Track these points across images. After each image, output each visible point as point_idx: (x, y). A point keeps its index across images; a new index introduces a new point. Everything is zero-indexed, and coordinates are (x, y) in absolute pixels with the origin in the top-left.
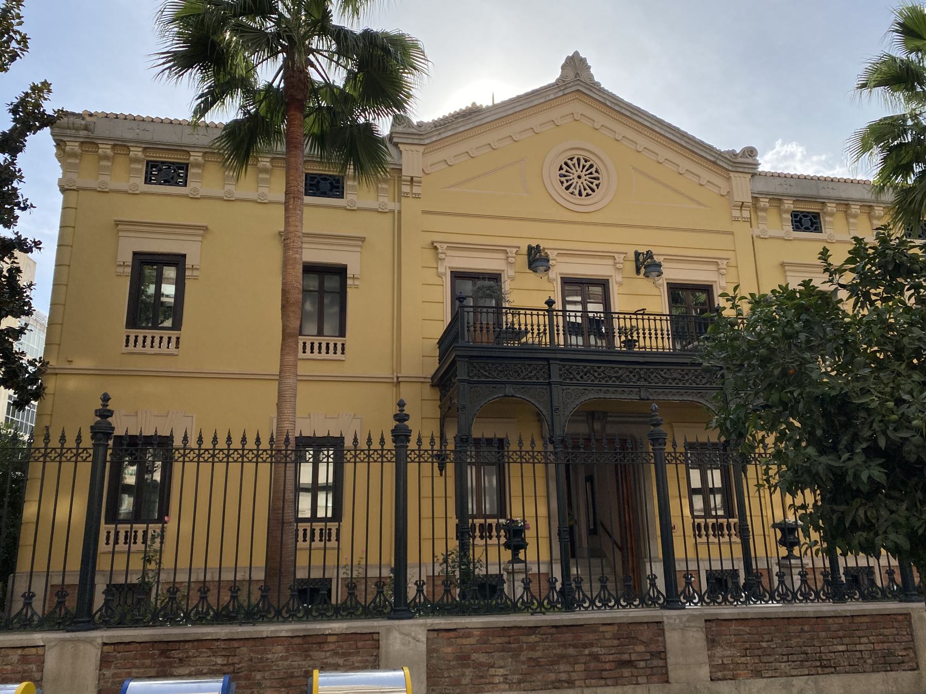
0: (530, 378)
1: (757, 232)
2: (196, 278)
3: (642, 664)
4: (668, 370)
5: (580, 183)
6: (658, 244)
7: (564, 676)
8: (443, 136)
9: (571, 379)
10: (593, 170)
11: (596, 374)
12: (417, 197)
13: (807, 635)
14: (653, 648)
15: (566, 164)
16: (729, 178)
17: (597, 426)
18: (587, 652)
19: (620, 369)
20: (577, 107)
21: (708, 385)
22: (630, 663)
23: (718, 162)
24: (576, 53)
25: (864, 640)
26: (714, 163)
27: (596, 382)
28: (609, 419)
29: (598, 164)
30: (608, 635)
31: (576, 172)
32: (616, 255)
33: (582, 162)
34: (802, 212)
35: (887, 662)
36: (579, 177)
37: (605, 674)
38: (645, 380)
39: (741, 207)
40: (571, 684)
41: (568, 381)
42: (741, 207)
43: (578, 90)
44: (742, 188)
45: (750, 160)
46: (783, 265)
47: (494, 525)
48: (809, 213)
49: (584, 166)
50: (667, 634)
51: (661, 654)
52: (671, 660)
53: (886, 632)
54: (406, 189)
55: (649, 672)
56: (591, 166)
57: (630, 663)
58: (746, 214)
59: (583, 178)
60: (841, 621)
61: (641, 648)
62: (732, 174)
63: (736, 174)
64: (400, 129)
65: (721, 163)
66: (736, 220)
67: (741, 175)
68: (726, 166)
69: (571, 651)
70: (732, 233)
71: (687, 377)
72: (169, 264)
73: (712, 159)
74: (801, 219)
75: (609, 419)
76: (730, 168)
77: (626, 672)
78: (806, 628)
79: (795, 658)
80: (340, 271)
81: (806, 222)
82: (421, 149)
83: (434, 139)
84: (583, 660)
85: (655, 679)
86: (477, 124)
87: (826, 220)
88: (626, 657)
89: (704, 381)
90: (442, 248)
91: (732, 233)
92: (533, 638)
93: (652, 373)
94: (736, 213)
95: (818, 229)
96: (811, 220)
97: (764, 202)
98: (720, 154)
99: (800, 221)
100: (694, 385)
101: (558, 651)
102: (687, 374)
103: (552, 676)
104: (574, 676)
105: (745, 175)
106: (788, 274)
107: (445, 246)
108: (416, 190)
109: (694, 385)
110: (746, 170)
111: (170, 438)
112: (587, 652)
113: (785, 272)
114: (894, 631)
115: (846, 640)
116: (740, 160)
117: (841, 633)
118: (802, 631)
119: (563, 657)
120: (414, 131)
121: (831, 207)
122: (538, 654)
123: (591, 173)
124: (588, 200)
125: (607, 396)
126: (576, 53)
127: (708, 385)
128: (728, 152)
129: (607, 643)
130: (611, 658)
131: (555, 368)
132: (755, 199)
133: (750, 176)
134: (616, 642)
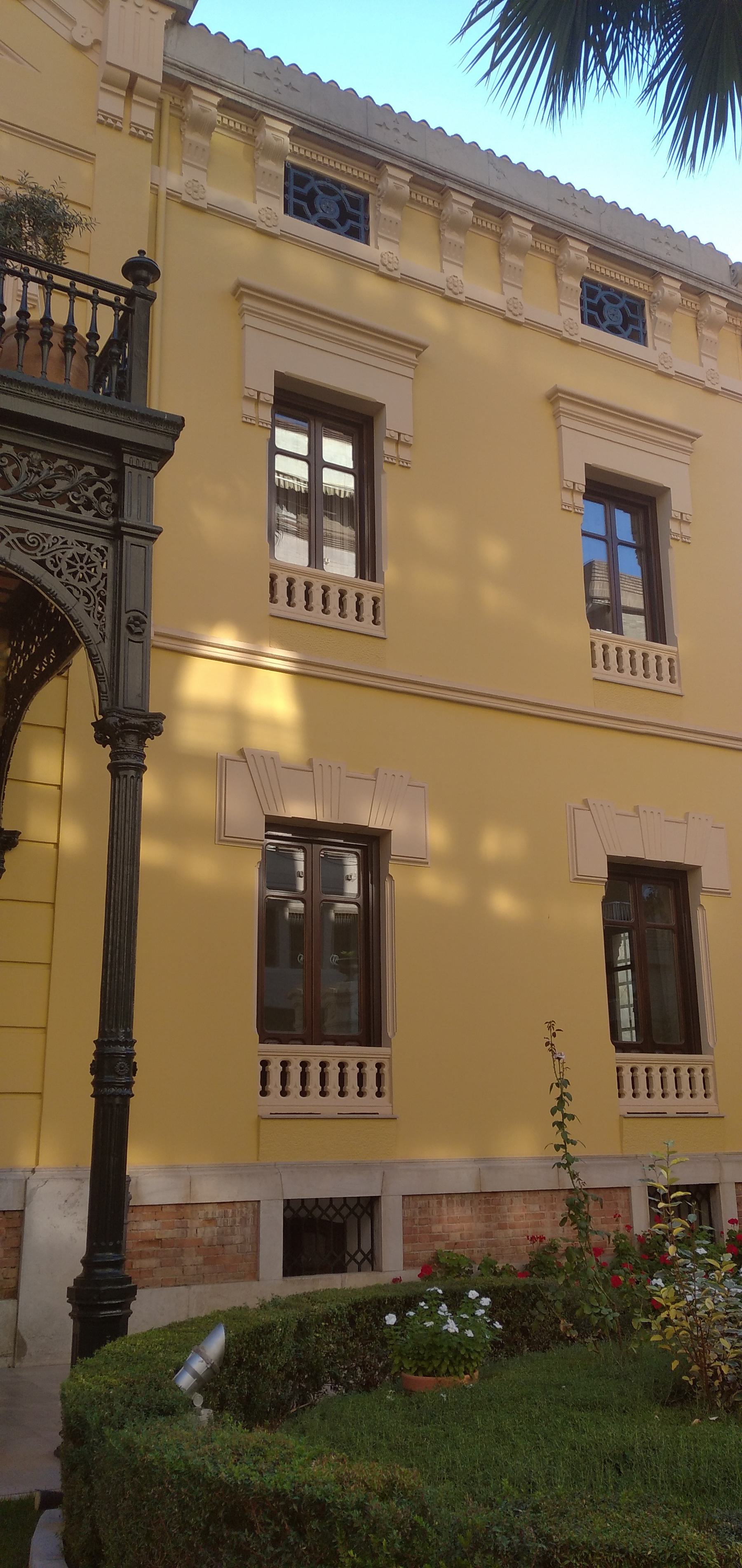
1: (174, 180)
34: (318, 177)
46: (240, 291)
48: (339, 184)
58: (145, 117)
66: (108, 122)
70: (88, 156)
74: (312, 194)
81: (327, 207)
87: (380, 214)
91: (88, 156)
94: (114, 105)
95: (359, 233)
96: (341, 204)
97: (205, 103)
99: (310, 198)
106: (248, 319)
113: (241, 314)
121: (396, 180)
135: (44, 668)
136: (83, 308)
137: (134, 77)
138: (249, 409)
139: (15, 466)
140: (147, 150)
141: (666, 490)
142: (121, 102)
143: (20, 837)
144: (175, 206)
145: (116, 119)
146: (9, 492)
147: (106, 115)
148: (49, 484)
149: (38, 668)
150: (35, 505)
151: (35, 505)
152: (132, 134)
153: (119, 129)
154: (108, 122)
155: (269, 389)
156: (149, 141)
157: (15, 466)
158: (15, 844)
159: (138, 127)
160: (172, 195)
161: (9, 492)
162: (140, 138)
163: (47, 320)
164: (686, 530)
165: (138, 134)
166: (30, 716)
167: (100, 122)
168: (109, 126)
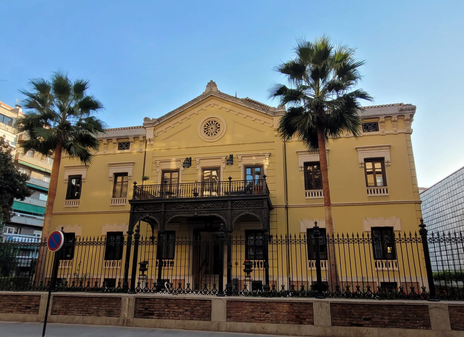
2: (85, 182)
3: (32, 308)
6: (236, 152)
7: (11, 310)
13: (85, 303)
14: (37, 304)
15: (217, 123)
18: (18, 303)
20: (212, 102)
22: (29, 308)
23: (268, 113)
24: (212, 81)
25: (104, 306)
29: (219, 122)
30: (25, 299)
31: (214, 127)
35: (110, 313)
37: (22, 310)
38: (197, 208)
40: (12, 312)
43: (212, 96)
46: (297, 152)
50: (41, 300)
51: (38, 306)
52: (40, 308)
53: (111, 303)
54: (148, 143)
55: (34, 311)
57: (29, 308)
60: (97, 299)
61: (33, 303)
64: (146, 122)
68: (271, 115)
69: (15, 303)
70: (274, 142)
72: (74, 178)
77: (28, 310)
78: (85, 300)
79: (79, 309)
80: (125, 174)
82: (153, 128)
84: (17, 305)
85: (35, 313)
88: (29, 306)
90: (158, 162)
92: (5, 298)
101: (11, 302)
103: (8, 310)
104: (14, 310)
111: (122, 232)
112: (18, 303)
114: (115, 303)
115: (98, 305)
116: (276, 111)
117: (96, 303)
118: (84, 301)
119: (12, 305)
122: (6, 303)
126: (212, 81)
129: (24, 301)
130: (25, 305)
134: (27, 301)
138: (300, 169)
141: (384, 158)
154: (276, 136)
155: (303, 165)
164: (389, 164)
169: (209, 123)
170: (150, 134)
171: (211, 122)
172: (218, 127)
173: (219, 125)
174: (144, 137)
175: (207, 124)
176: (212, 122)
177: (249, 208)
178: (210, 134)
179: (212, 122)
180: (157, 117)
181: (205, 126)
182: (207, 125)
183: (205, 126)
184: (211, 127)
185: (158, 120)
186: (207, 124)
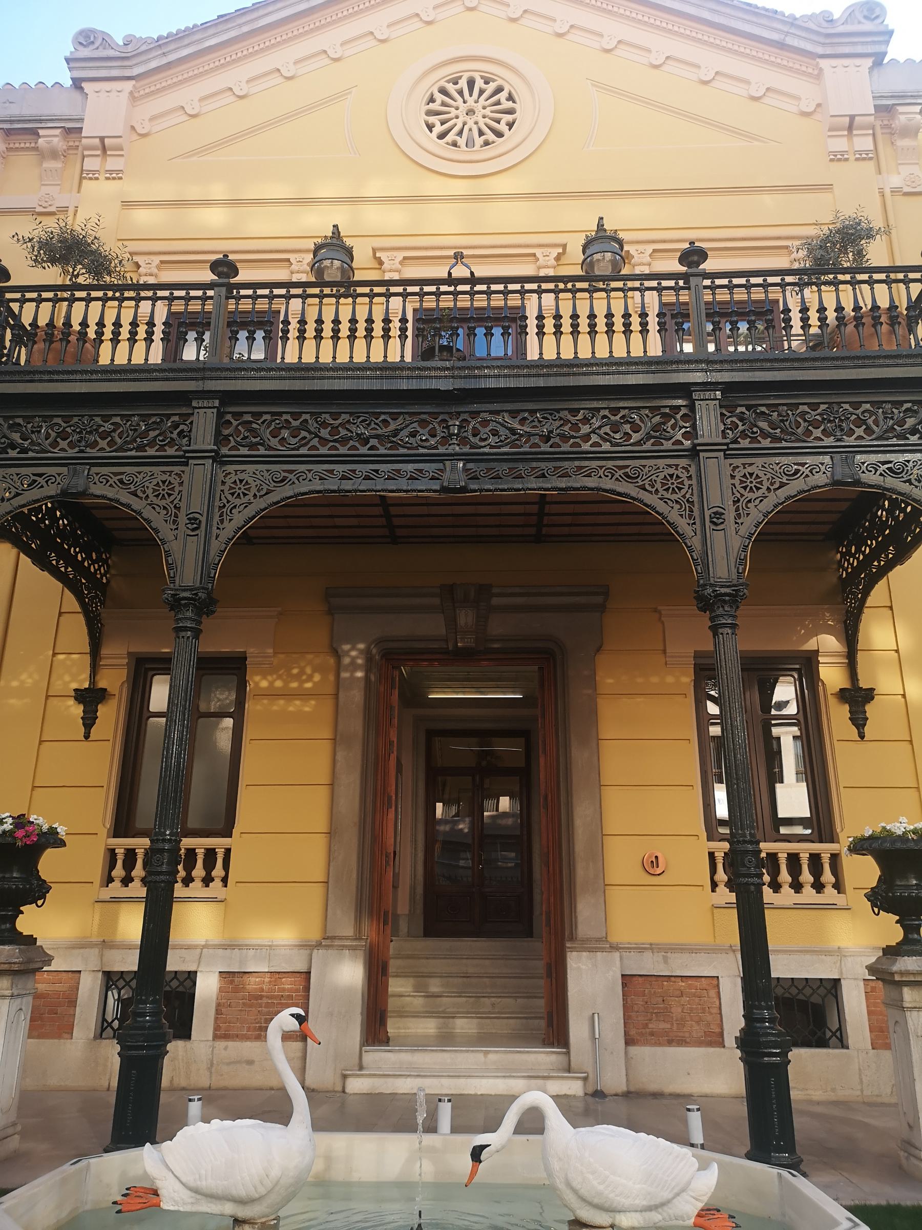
0: (141, 448)
1: (895, 181)
4: (533, 412)
5: (470, 123)
8: (172, 57)
9: (252, 446)
10: (503, 96)
11: (324, 433)
12: (115, 175)
16: (818, 76)
17: (466, 618)
19: (395, 416)
21: (648, 446)
23: (789, 41)
26: (781, 46)
27: (323, 451)
28: (495, 601)
29: (512, 83)
32: (539, 252)
33: (479, 83)
36: (470, 112)
38: (464, 441)
39: (850, 128)
41: (244, 451)
42: (850, 128)
44: (850, 88)
45: (868, 26)
47: (200, 853)
49: (482, 92)
54: (91, 164)
56: (499, 90)
58: (865, 143)
59: (480, 112)
62: (824, 63)
63: (834, 62)
65: (795, 42)
66: (838, 158)
67: (846, 62)
68: (809, 47)
71: (585, 429)
73: (775, 36)
75: (495, 601)
76: (820, 50)
82: (128, 86)
83: (153, 64)
86: (245, 29)
89: (635, 437)
93: (485, 423)
94: (840, 144)
98: (792, 22)
100: (606, 446)
102: (586, 421)
105: (858, 61)
107: (156, 260)
108: (112, 163)
109: (606, 446)
110: (860, 49)
120: (111, 53)
123: (482, 92)
124: (489, 152)
125: (347, 485)
127: (648, 446)
128: (812, 17)
131: (203, 425)
132: (885, 110)
133: (869, 62)
135: (882, 563)
136: (881, 290)
137: (852, 118)
139: (874, 417)
140: (871, 165)
142: (845, 139)
143: (875, 692)
144: (900, 199)
145: (842, 153)
146: (874, 436)
147: (835, 153)
148: (901, 423)
149: (876, 563)
150: (894, 441)
151: (894, 441)
152: (857, 159)
153: (847, 160)
154: (838, 158)
156: (871, 159)
157: (874, 417)
158: (873, 698)
159: (860, 152)
160: (895, 191)
161: (874, 436)
162: (864, 159)
163: (875, 307)
165: (862, 157)
166: (870, 602)
167: (831, 160)
168: (839, 160)
169: (451, 88)
170: (105, 110)
171: (463, 84)
172: (504, 112)
173: (510, 98)
174: (73, 132)
175: (443, 91)
176: (471, 83)
177: (850, 441)
178: (462, 141)
179: (471, 83)
180: (153, 28)
181: (432, 100)
182: (439, 97)
183: (432, 100)
184: (463, 108)
185: (162, 43)
186: (443, 91)
